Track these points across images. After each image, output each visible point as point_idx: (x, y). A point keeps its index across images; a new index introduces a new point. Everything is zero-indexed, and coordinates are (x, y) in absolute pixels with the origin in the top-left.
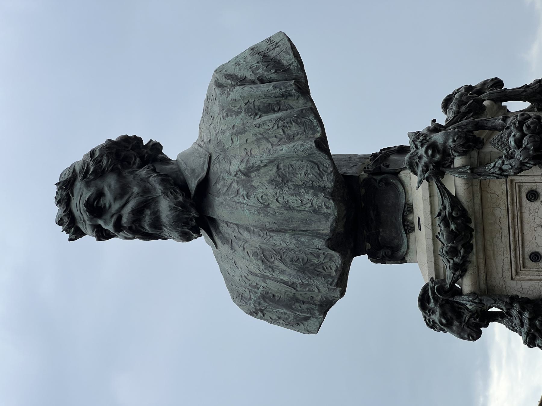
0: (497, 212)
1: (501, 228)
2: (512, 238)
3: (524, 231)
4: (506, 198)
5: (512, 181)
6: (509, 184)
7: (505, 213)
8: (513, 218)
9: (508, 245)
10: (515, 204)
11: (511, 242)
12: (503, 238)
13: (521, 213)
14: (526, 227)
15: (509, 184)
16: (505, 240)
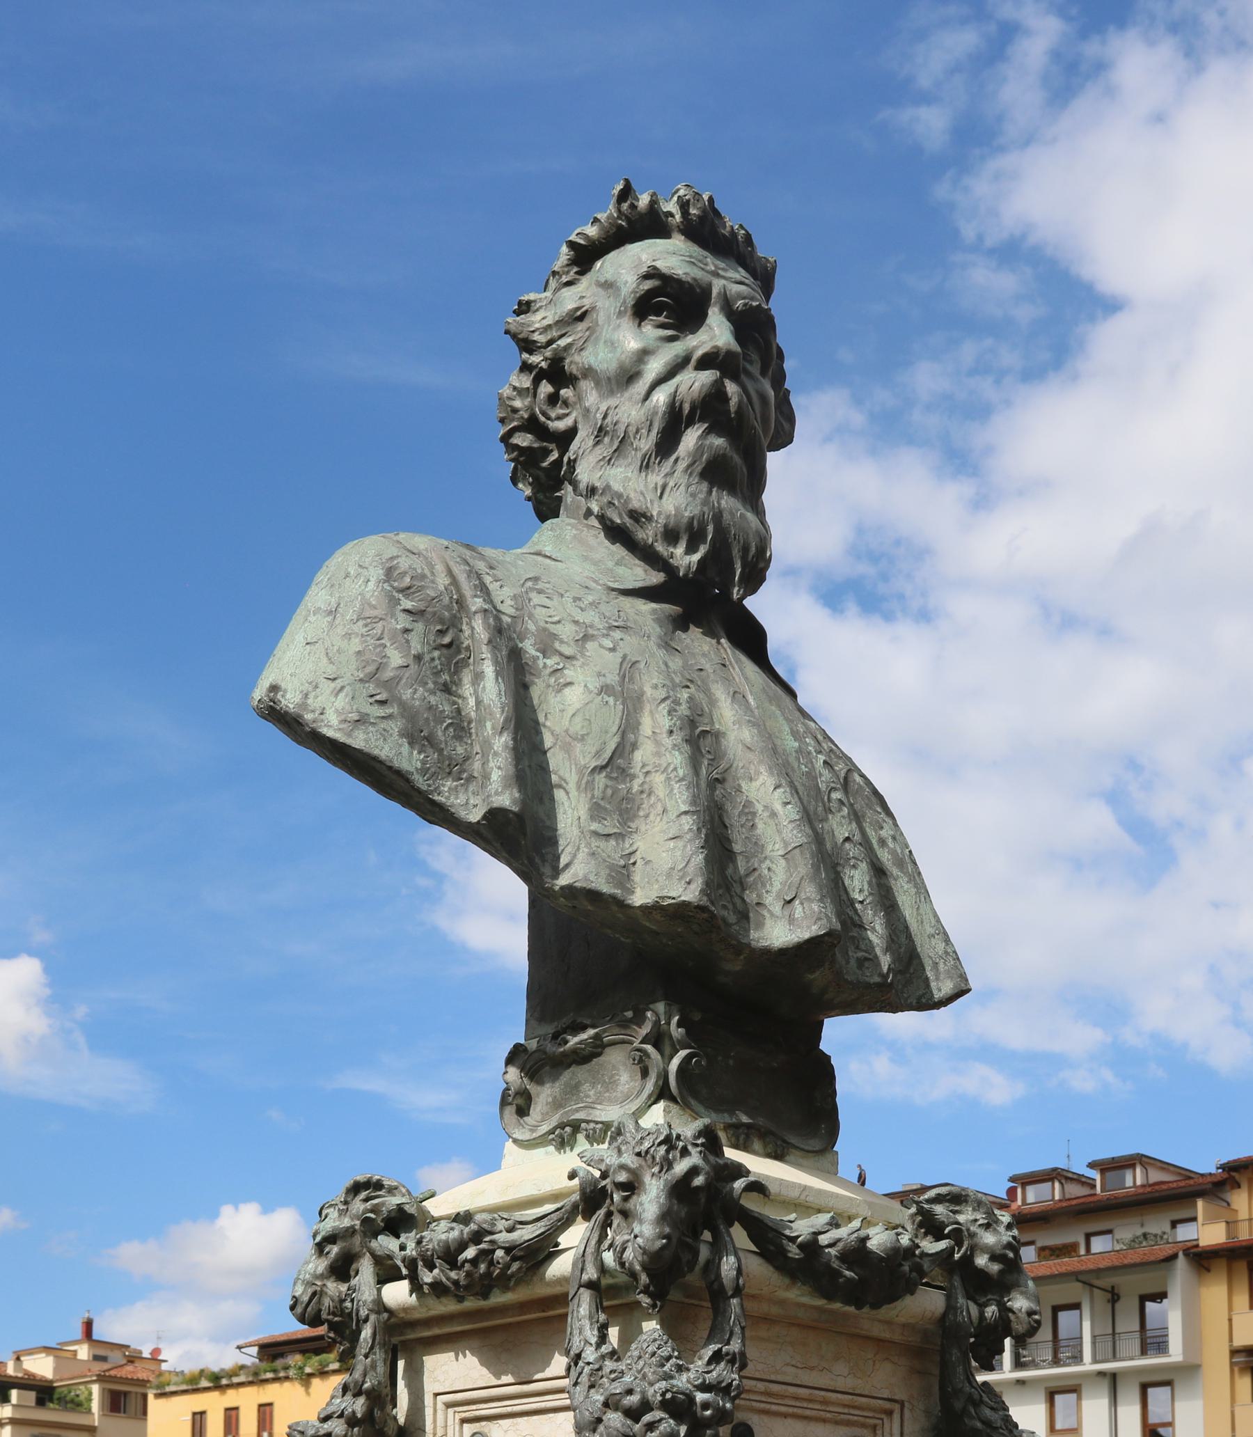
0: (841, 1368)
1: (812, 1368)
2: (792, 1389)
3: (789, 1421)
4: (866, 1393)
5: (890, 1413)
6: (887, 1405)
7: (840, 1384)
8: (825, 1402)
9: (780, 1378)
10: (846, 1411)
11: (784, 1387)
12: (793, 1370)
13: (824, 1421)
14: (799, 1426)
15: (887, 1405)
16: (790, 1375)
